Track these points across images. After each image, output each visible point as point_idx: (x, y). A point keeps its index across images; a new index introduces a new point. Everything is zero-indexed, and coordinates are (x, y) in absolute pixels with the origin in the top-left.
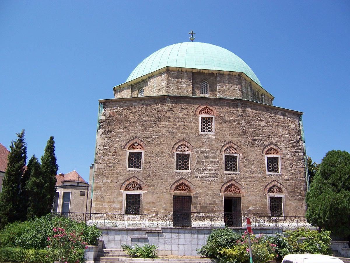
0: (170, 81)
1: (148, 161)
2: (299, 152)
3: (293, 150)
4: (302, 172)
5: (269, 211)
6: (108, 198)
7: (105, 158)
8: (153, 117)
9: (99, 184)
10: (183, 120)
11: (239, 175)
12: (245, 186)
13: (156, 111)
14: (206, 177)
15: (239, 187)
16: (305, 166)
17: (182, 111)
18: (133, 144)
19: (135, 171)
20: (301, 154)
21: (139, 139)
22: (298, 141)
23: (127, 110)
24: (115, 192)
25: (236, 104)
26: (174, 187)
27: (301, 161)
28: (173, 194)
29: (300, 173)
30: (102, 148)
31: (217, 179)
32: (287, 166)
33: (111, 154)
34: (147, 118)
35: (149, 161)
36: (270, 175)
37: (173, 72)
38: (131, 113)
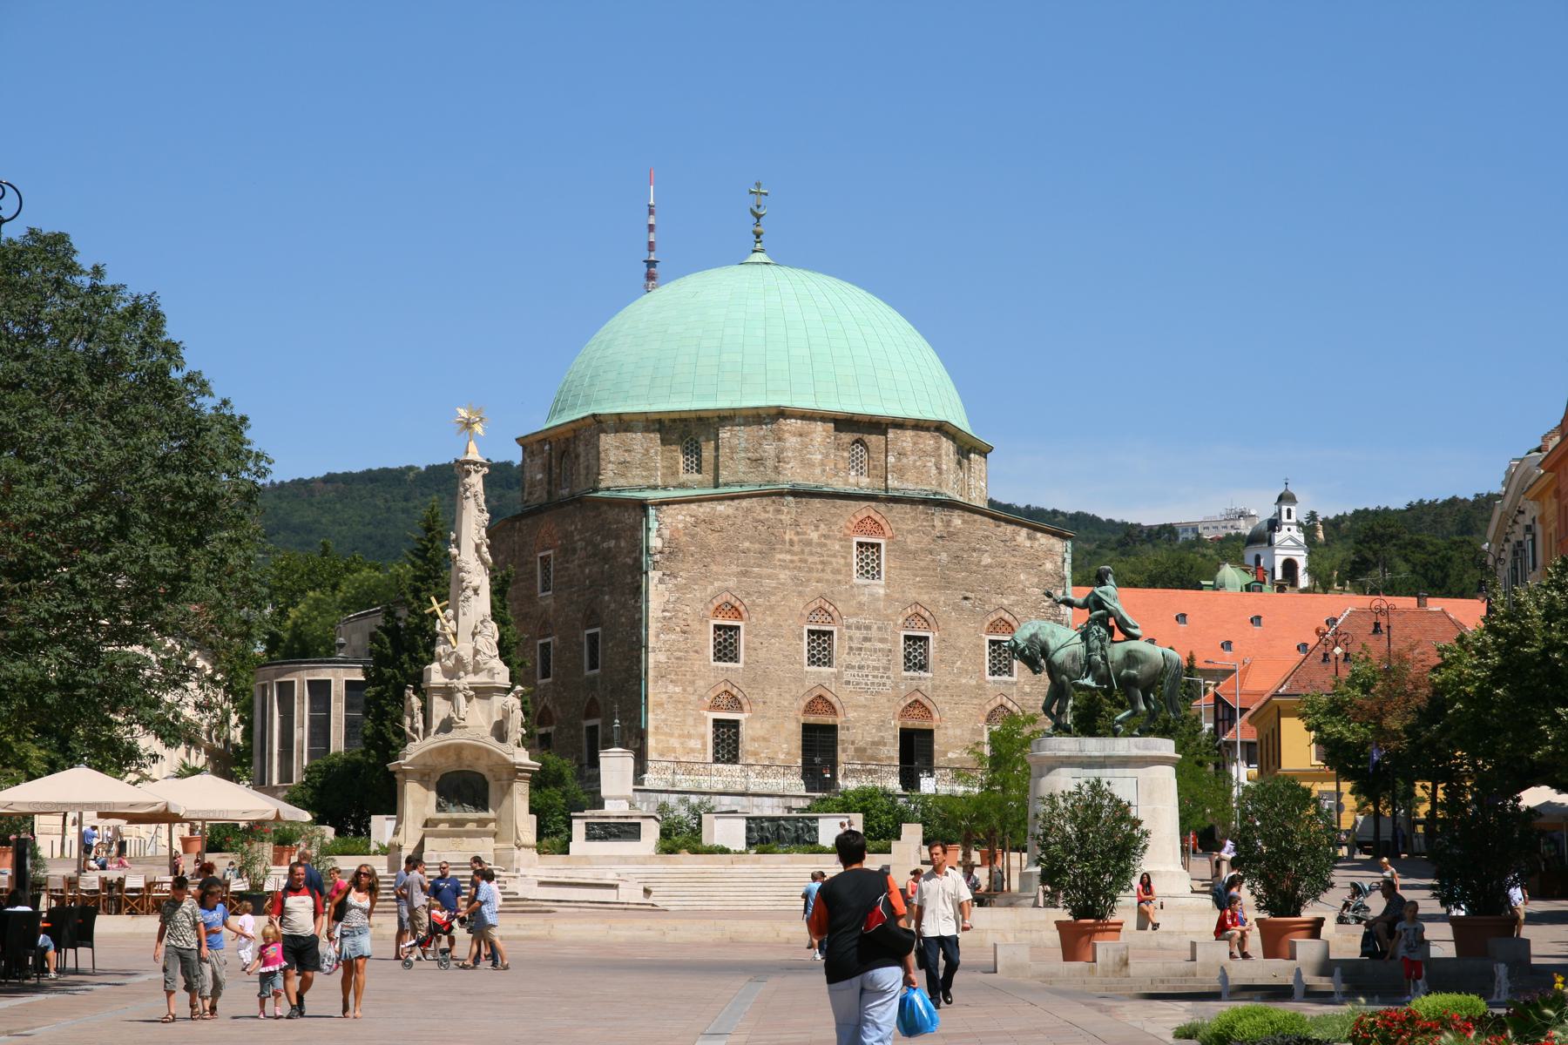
0: (788, 445)
1: (752, 645)
7: (668, 637)
8: (760, 543)
10: (819, 550)
11: (932, 679)
14: (866, 684)
15: (931, 707)
17: (817, 527)
26: (803, 704)
28: (802, 721)
30: (661, 615)
33: (678, 629)
34: (747, 544)
37: (793, 421)
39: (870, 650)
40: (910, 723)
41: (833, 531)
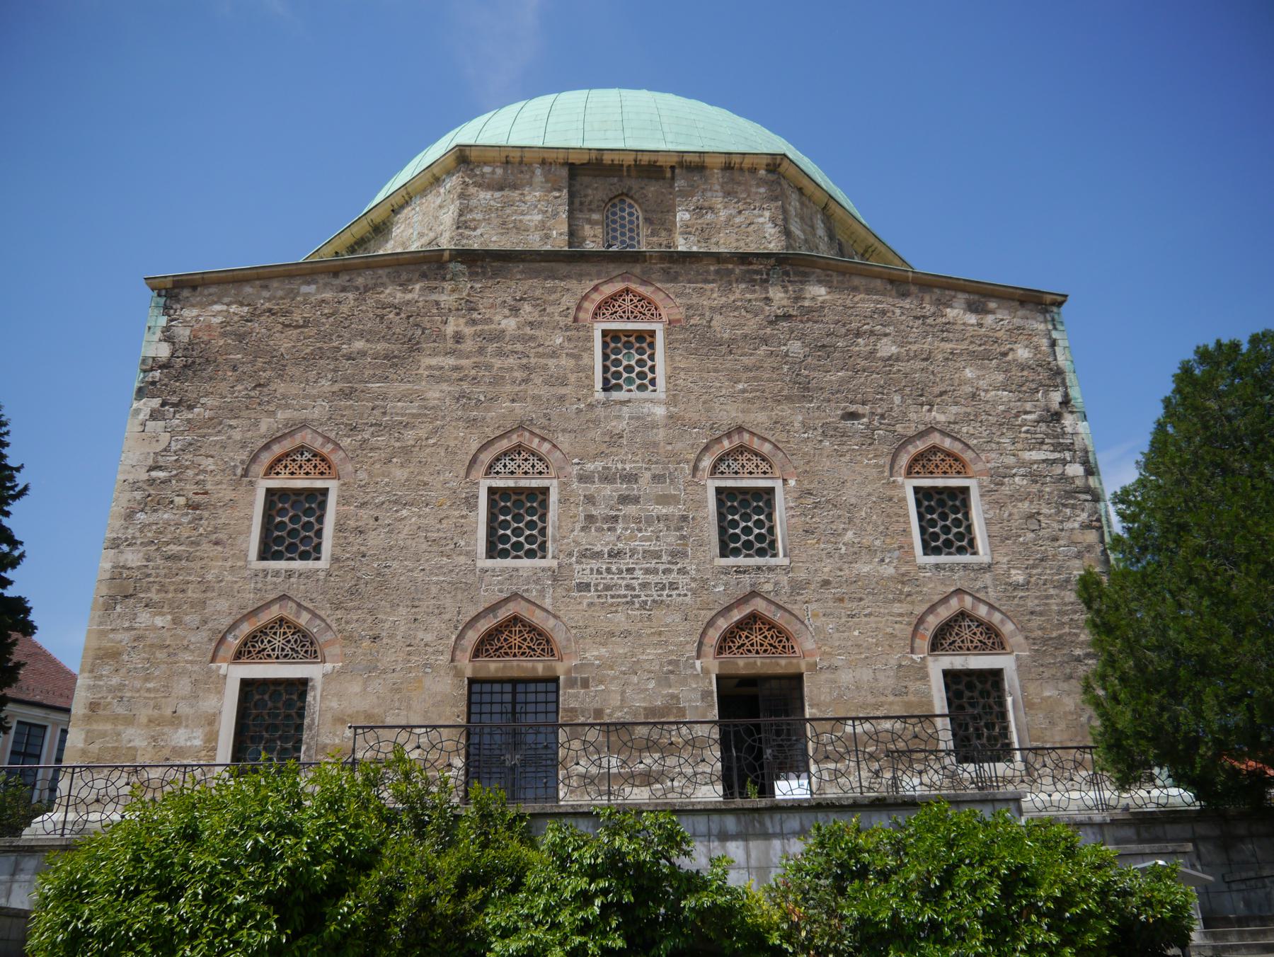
0: (473, 202)
1: (352, 523)
2: (1064, 462)
3: (1035, 455)
4: (1089, 548)
5: (946, 739)
6: (152, 703)
9: (112, 641)
10: (519, 347)
11: (787, 570)
12: (818, 624)
13: (403, 315)
14: (628, 587)
15: (791, 626)
16: (1099, 520)
18: (287, 455)
19: (290, 574)
20: (1076, 470)
21: (316, 431)
22: (1056, 417)
23: (273, 314)
24: (184, 672)
25: (757, 272)
26: (472, 637)
27: (1076, 498)
28: (469, 673)
29: (1079, 555)
30: (145, 476)
31: (679, 595)
32: (1014, 524)
33: (181, 501)
34: (359, 345)
35: (359, 524)
36: (937, 567)
37: (487, 169)
38: (289, 326)
39: (638, 520)
40: (741, 663)
41: (551, 315)
